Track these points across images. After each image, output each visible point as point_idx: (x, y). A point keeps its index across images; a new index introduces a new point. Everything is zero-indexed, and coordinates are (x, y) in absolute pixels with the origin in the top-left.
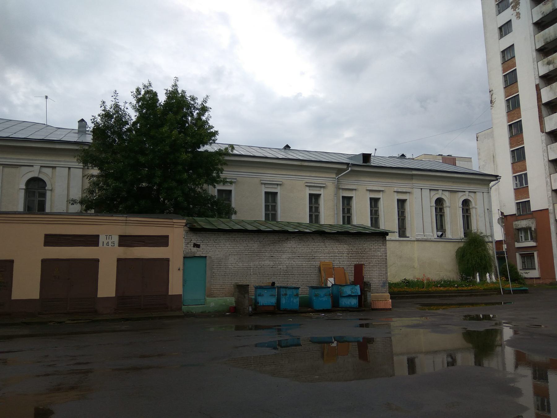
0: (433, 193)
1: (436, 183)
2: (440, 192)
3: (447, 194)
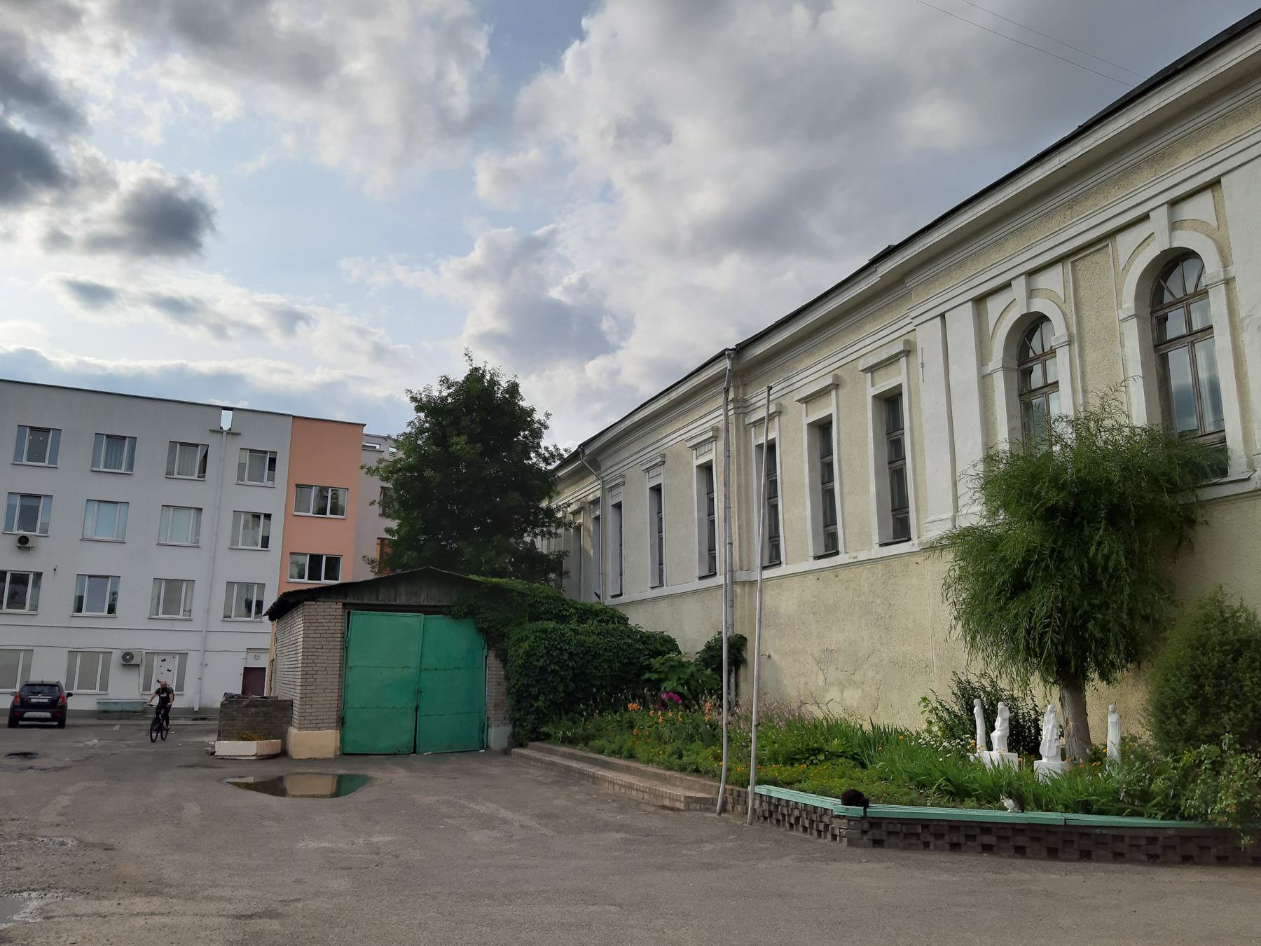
0: (994, 306)
1: (995, 257)
2: (1019, 287)
3: (1053, 280)
